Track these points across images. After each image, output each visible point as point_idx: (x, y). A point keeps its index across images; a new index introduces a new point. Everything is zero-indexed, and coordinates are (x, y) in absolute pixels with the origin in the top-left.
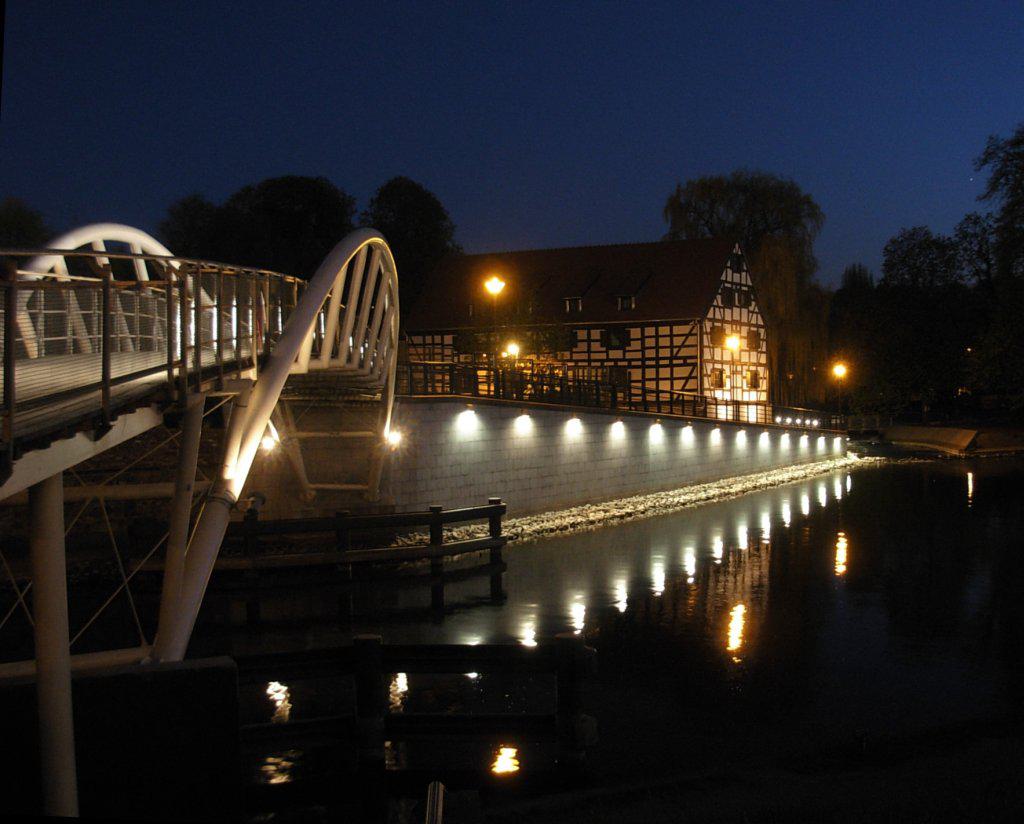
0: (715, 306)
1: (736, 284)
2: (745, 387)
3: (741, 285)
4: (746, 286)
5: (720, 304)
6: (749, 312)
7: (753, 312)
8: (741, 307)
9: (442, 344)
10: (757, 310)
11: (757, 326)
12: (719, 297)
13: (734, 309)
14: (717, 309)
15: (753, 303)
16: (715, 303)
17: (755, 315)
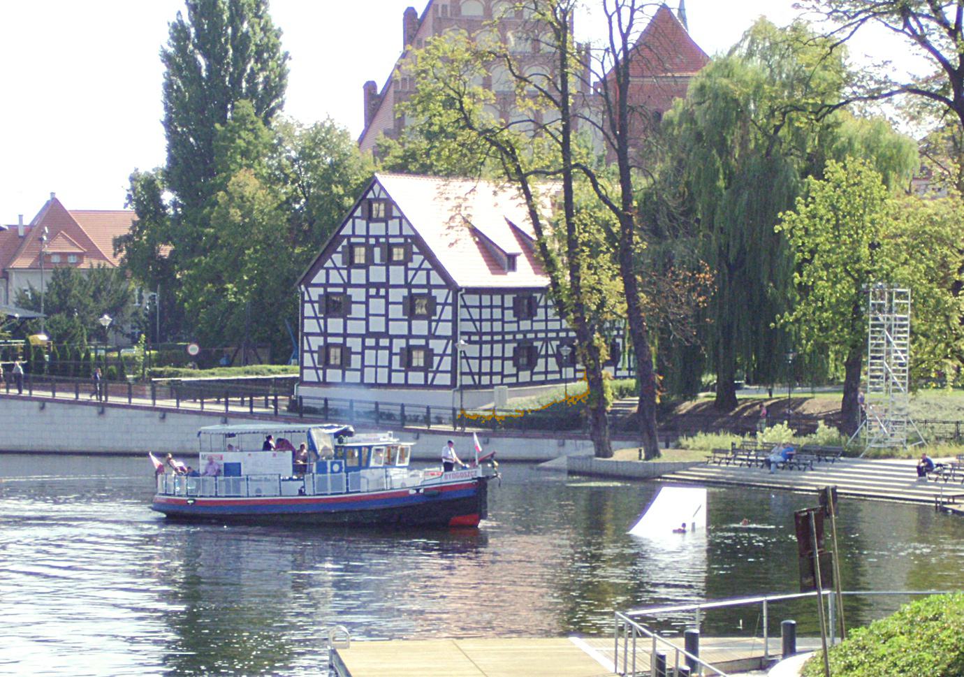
0: (328, 270)
1: (377, 237)
2: (396, 365)
3: (387, 236)
4: (401, 235)
5: (339, 264)
6: (407, 269)
7: (420, 269)
8: (388, 261)
9: (503, 308)
10: (427, 265)
11: (428, 286)
12: (338, 258)
13: (371, 268)
14: (333, 273)
15: (417, 259)
16: (329, 264)
17: (422, 274)
